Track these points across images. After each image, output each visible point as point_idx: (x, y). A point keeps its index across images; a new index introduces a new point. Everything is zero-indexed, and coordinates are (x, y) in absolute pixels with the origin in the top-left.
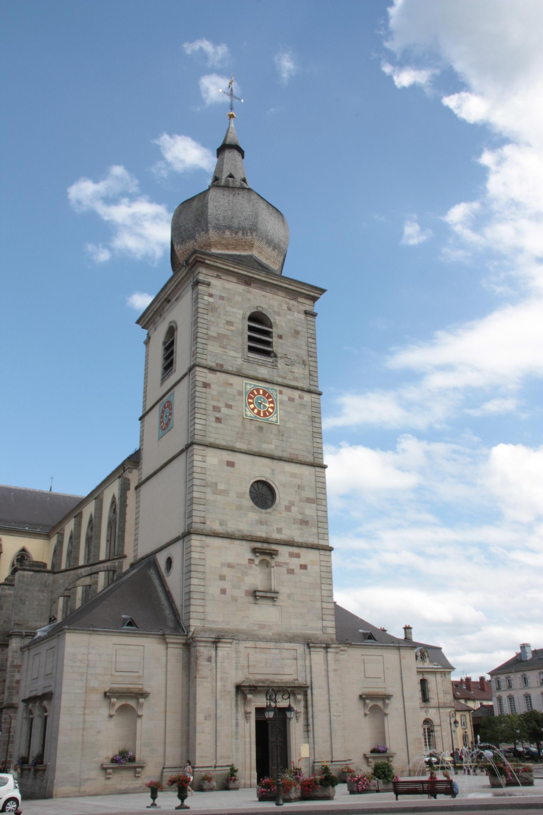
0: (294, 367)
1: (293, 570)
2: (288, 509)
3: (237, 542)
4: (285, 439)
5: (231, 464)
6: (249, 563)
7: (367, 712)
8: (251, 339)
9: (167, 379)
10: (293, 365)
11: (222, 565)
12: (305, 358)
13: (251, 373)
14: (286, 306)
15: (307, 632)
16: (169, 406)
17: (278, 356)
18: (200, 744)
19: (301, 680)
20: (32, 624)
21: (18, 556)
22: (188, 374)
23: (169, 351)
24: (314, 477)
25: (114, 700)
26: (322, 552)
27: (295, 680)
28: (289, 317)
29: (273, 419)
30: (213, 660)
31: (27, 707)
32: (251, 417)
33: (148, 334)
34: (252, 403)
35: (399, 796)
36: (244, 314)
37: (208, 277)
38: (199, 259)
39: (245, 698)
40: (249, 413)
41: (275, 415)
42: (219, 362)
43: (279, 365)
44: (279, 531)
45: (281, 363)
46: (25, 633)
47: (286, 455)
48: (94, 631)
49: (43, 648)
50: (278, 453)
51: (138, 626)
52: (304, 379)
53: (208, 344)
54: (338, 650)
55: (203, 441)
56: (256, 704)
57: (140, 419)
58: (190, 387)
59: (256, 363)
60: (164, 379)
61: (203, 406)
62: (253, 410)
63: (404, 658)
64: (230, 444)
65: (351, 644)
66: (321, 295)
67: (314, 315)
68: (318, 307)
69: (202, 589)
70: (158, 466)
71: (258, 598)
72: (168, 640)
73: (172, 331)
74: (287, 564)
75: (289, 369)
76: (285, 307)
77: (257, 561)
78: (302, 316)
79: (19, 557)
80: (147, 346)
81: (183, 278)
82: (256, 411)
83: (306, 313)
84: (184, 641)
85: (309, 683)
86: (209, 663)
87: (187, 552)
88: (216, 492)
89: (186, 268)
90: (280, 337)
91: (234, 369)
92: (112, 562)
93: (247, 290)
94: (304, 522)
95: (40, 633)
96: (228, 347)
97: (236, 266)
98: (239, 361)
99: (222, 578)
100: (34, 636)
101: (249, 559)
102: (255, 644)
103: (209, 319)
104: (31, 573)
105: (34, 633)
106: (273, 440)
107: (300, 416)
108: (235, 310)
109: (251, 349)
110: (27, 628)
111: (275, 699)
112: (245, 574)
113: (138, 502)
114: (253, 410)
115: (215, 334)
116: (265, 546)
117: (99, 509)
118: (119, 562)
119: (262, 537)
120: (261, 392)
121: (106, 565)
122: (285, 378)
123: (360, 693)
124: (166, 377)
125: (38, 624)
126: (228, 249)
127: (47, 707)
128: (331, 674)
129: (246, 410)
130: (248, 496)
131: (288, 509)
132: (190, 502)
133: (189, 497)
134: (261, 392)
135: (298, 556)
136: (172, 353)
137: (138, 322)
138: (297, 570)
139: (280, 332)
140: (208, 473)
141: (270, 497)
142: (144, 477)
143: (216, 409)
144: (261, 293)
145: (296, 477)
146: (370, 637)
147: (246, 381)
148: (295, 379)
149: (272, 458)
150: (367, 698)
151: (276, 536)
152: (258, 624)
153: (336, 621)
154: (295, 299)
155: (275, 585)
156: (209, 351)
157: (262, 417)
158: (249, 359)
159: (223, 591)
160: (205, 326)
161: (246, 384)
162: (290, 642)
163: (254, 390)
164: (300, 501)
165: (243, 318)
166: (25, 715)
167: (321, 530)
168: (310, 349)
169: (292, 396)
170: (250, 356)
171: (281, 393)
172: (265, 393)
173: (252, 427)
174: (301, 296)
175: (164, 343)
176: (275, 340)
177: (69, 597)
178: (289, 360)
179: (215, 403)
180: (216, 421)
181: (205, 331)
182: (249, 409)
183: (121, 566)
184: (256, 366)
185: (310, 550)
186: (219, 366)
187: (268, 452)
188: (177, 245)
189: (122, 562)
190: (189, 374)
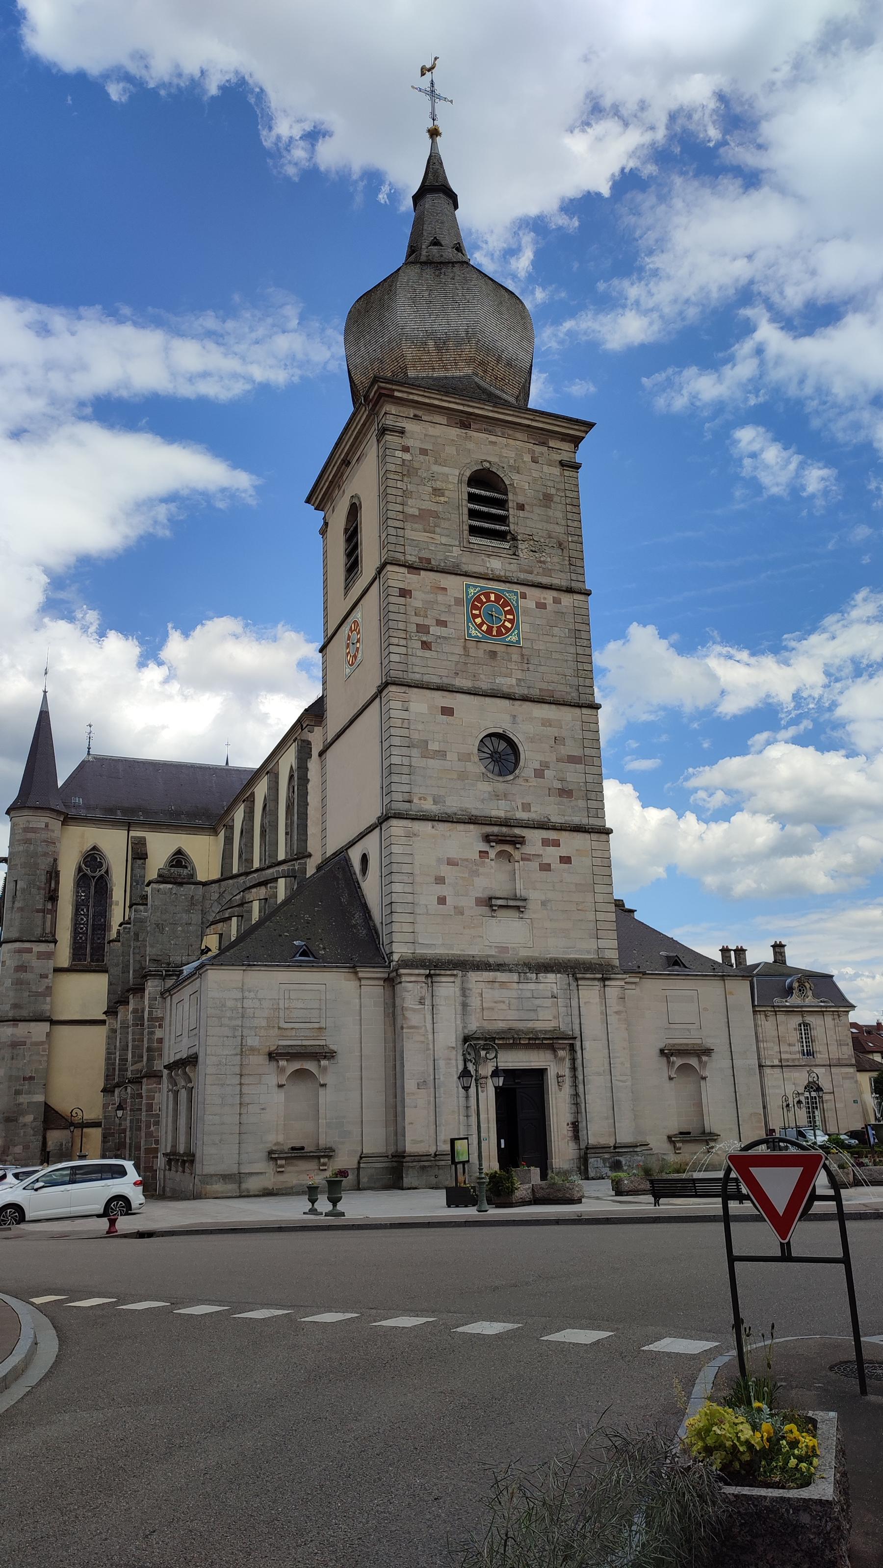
1: (549, 865)
2: (539, 774)
3: (461, 827)
4: (531, 667)
5: (447, 711)
8: (473, 514)
9: (352, 586)
11: (439, 860)
12: (563, 537)
14: (530, 456)
15: (572, 956)
20: (176, 959)
21: (172, 861)
22: (378, 579)
24: (579, 723)
25: (282, 1063)
26: (594, 836)
28: (535, 474)
30: (428, 1002)
31: (170, 1076)
32: (477, 637)
33: (324, 518)
34: (479, 616)
36: (461, 475)
37: (400, 419)
40: (473, 632)
41: (516, 632)
44: (526, 807)
48: (249, 965)
49: (186, 991)
57: (321, 651)
59: (483, 552)
61: (401, 626)
62: (480, 626)
63: (731, 993)
64: (446, 681)
65: (644, 974)
66: (587, 432)
67: (576, 467)
69: (409, 899)
71: (494, 908)
72: (361, 975)
73: (354, 510)
76: (527, 458)
77: (492, 854)
78: (556, 471)
79: (174, 863)
80: (325, 537)
81: (364, 425)
82: (484, 628)
83: (562, 464)
84: (386, 976)
85: (577, 1033)
86: (423, 1006)
87: (385, 847)
90: (521, 507)
95: (187, 970)
98: (456, 551)
99: (440, 880)
100: (178, 976)
101: (480, 852)
104: (170, 886)
107: (556, 630)
108: (446, 470)
112: (476, 873)
113: (323, 775)
114: (480, 626)
116: (504, 830)
117: (274, 787)
120: (493, 597)
123: (662, 1046)
127: (191, 1075)
128: (612, 1019)
129: (468, 627)
130: (476, 759)
131: (539, 774)
132: (388, 771)
134: (493, 597)
135: (556, 843)
136: (356, 547)
137: (308, 501)
138: (556, 865)
139: (521, 499)
142: (330, 737)
143: (423, 629)
145: (550, 726)
146: (675, 962)
148: (548, 572)
154: (543, 444)
155: (521, 891)
156: (408, 539)
157: (494, 636)
158: (471, 546)
159: (442, 900)
161: (468, 586)
164: (558, 760)
165: (460, 481)
166: (170, 1087)
169: (542, 601)
171: (524, 596)
174: (553, 438)
175: (346, 530)
179: (420, 620)
181: (400, 508)
182: (473, 626)
183: (304, 871)
185: (575, 834)
186: (424, 561)
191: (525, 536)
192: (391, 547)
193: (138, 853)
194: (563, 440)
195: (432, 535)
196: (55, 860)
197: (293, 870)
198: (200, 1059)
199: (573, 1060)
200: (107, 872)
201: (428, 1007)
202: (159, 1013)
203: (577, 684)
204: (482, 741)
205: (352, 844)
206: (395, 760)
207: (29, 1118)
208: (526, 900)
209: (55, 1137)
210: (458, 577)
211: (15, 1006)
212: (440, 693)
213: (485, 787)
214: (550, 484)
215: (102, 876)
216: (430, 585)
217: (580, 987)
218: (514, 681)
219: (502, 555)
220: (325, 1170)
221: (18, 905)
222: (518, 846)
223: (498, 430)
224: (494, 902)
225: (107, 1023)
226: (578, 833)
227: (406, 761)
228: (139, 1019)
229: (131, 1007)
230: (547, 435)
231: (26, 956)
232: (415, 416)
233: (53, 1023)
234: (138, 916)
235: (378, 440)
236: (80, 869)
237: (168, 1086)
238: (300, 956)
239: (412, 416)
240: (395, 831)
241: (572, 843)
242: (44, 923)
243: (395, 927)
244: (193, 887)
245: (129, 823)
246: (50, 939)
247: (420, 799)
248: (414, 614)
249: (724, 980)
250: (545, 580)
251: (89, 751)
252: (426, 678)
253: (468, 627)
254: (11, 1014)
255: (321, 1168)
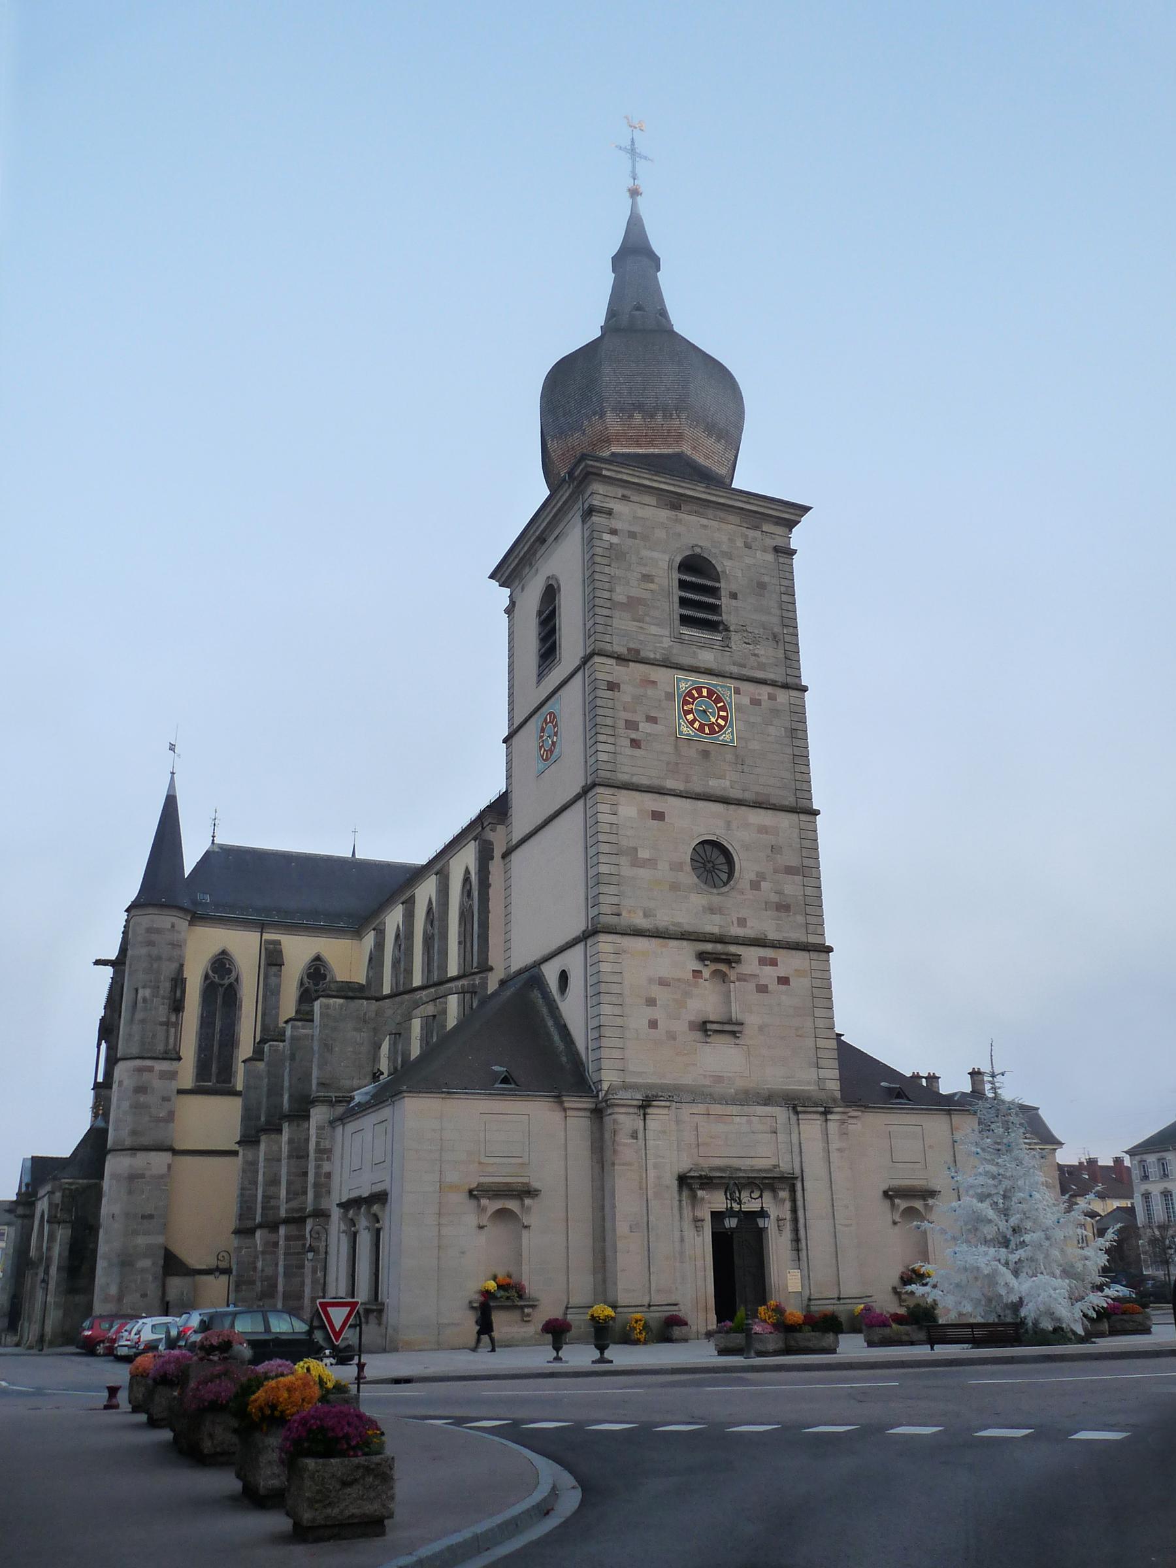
0: (758, 647)
1: (766, 986)
2: (755, 886)
3: (673, 943)
5: (658, 816)
6: (694, 977)
7: (898, 1219)
8: (683, 602)
10: (756, 643)
11: (650, 981)
13: (686, 661)
16: (554, 720)
17: (731, 629)
18: (623, 1270)
19: (785, 1167)
20: (346, 1083)
21: (309, 968)
22: (582, 668)
23: (548, 628)
25: (484, 1202)
26: (814, 955)
27: (775, 1166)
28: (748, 561)
29: (726, 736)
30: (641, 1135)
35: (936, 1346)
36: (671, 561)
38: (591, 470)
39: (694, 1197)
40: (685, 729)
42: (632, 646)
43: (733, 645)
44: (742, 922)
45: (736, 640)
46: (336, 1097)
47: (748, 796)
48: (448, 1093)
49: (368, 1121)
50: (736, 794)
51: (519, 1084)
52: (776, 666)
53: (613, 616)
54: (845, 1117)
55: (612, 779)
56: (712, 1206)
57: (505, 741)
58: (587, 689)
59: (695, 643)
60: (541, 676)
61: (609, 722)
62: (692, 723)
64: (656, 782)
68: (798, 538)
69: (619, 1021)
70: (539, 821)
71: (709, 1033)
72: (567, 1105)
73: (551, 593)
74: (756, 976)
75: (750, 650)
76: (740, 543)
77: (706, 973)
78: (770, 557)
80: (511, 617)
81: (565, 503)
82: (697, 725)
84: (592, 1106)
85: (797, 1172)
86: (635, 1141)
87: (591, 964)
88: (636, 863)
89: (570, 485)
90: (734, 596)
91: (658, 657)
92: (470, 978)
93: (674, 517)
94: (783, 907)
95: (359, 1097)
96: (647, 619)
97: (655, 478)
98: (667, 642)
99: (651, 1002)
100: (349, 1102)
101: (693, 971)
102: (708, 1109)
103: (613, 574)
104: (341, 1001)
105: (351, 1097)
106: (728, 772)
107: (772, 730)
108: (655, 555)
109: (685, 620)
110: (339, 1089)
111: (739, 1198)
114: (692, 723)
115: (625, 601)
116: (719, 947)
118: (481, 978)
119: (713, 934)
120: (705, 693)
121: (460, 983)
122: (743, 666)
123: (885, 1187)
124: (545, 672)
125: (356, 1083)
126: (639, 445)
127: (380, 1214)
128: (834, 1156)
129: (680, 724)
130: (688, 868)
131: (755, 886)
133: (592, 873)
134: (705, 693)
135: (773, 963)
136: (553, 631)
137: (492, 577)
138: (773, 986)
139: (734, 587)
140: (620, 832)
141: (725, 868)
143: (632, 725)
144: (699, 522)
145: (767, 833)
146: (899, 1094)
147: (678, 675)
148: (762, 667)
149: (725, 801)
150: (897, 1196)
151: (736, 931)
152: (710, 1076)
153: (841, 1069)
154: (757, 528)
155: (736, 1013)
158: (683, 637)
159: (653, 1024)
160: (607, 586)
161: (679, 680)
162: (765, 1105)
163: (692, 689)
164: (776, 871)
165: (670, 567)
166: (343, 1227)
167: (811, 919)
168: (785, 614)
169: (757, 697)
170: (684, 632)
171: (737, 691)
172: (711, 693)
173: (692, 752)
175: (540, 613)
176: (725, 602)
177: (400, 1035)
178: (750, 635)
179: (629, 716)
180: (632, 746)
181: (606, 595)
182: (685, 723)
183: (484, 985)
184: (694, 648)
187: (719, 793)
188: (552, 440)
189: (486, 978)
190: (584, 669)
191: (738, 627)
192: (598, 636)
193: (273, 959)
194: (777, 524)
195: (641, 624)
196: (182, 965)
197: (474, 985)
198: (393, 1197)
199: (794, 1200)
200: (237, 980)
201: (641, 1142)
202: (326, 1144)
203: (794, 787)
204: (694, 849)
205: (546, 959)
206: (603, 869)
207: (146, 1263)
208: (742, 1024)
209: (176, 1285)
210: (669, 670)
211: (134, 1133)
212: (650, 795)
213: (698, 900)
214: (763, 571)
215: (231, 985)
216: (639, 678)
217: (800, 1121)
218: (728, 783)
219: (715, 647)
220: (529, 1321)
221: (139, 1015)
222: (733, 965)
223: (710, 512)
224: (709, 1026)
225: (241, 1154)
226: (798, 951)
227: (613, 869)
228: (299, 1153)
229: (285, 1137)
230: (760, 518)
231: (146, 1075)
232: (623, 496)
233: (175, 1152)
234: (295, 1034)
235: (583, 521)
236: (207, 977)
237: (339, 1227)
238: (501, 1083)
239: (620, 496)
240: (603, 947)
241: (791, 962)
242: (167, 1038)
243: (605, 1053)
244: (365, 1002)
245: (263, 924)
246: (174, 1056)
247: (630, 912)
248: (622, 709)
249: (950, 1115)
250: (760, 675)
251: (213, 840)
252: (635, 780)
253: (680, 724)
254: (128, 1142)
255: (525, 1319)
